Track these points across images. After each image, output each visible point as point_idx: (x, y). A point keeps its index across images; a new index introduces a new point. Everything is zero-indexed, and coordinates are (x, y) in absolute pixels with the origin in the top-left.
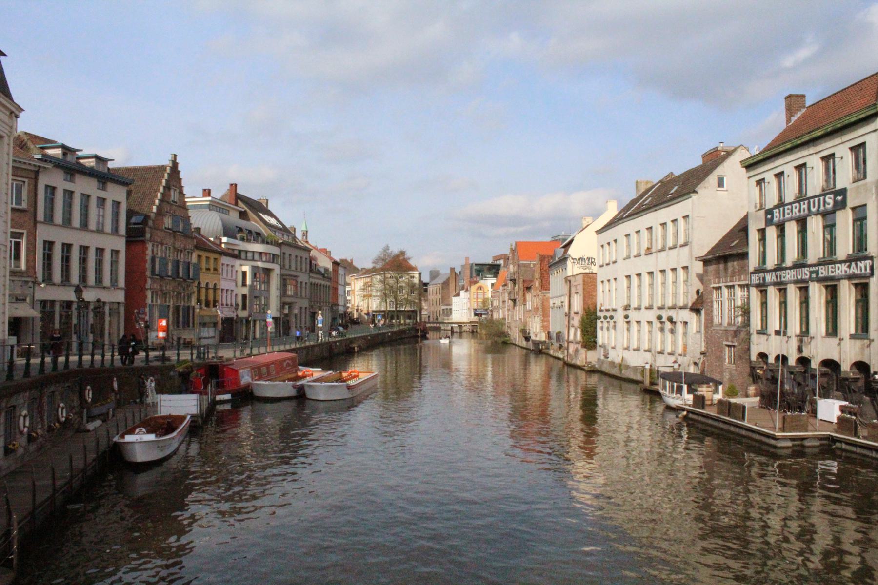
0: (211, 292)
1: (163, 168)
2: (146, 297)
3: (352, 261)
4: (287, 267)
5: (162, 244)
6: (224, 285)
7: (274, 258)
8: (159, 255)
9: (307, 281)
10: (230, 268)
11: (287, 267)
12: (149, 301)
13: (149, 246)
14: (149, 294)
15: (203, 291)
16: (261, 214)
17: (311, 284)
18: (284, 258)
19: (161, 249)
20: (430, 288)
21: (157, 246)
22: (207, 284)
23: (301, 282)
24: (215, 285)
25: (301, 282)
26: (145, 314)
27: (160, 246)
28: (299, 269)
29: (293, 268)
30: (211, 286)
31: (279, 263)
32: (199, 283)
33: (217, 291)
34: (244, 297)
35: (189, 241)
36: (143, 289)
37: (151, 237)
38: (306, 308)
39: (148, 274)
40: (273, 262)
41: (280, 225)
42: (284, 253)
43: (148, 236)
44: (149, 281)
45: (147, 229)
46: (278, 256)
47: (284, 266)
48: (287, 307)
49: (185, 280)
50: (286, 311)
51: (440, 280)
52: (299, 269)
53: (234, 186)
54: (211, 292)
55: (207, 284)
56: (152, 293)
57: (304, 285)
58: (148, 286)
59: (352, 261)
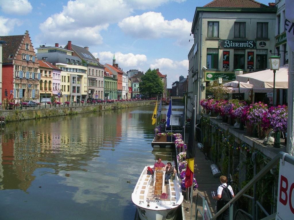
0: (48, 84)
1: (23, 36)
2: (13, 86)
3: (143, 72)
4: (91, 74)
5: (21, 66)
6: (53, 81)
7: (84, 71)
8: (20, 70)
9: (103, 80)
10: (58, 75)
11: (91, 74)
12: (14, 87)
13: (15, 67)
14: (14, 85)
15: (43, 84)
16: (83, 54)
17: (105, 81)
18: (89, 71)
19: (21, 68)
20: (180, 85)
21: (18, 67)
22: (46, 81)
23: (99, 81)
24: (50, 82)
25: (99, 81)
26: (13, 92)
27: (20, 67)
28: (98, 76)
29: (95, 74)
30: (48, 82)
31: (87, 73)
32: (41, 81)
33: (51, 84)
34: (68, 86)
35: (36, 64)
36: (12, 83)
37: (15, 63)
38: (102, 91)
39: (14, 77)
40: (83, 73)
41: (91, 57)
42: (90, 69)
43: (14, 62)
44: (14, 80)
45: (14, 60)
46: (86, 70)
47: (90, 74)
48: (90, 91)
49: (33, 80)
50: (90, 92)
51: (183, 81)
52: (98, 76)
53: (69, 42)
54: (48, 84)
55: (46, 81)
56: (16, 84)
57: (101, 82)
58: (14, 82)
59: (143, 72)
